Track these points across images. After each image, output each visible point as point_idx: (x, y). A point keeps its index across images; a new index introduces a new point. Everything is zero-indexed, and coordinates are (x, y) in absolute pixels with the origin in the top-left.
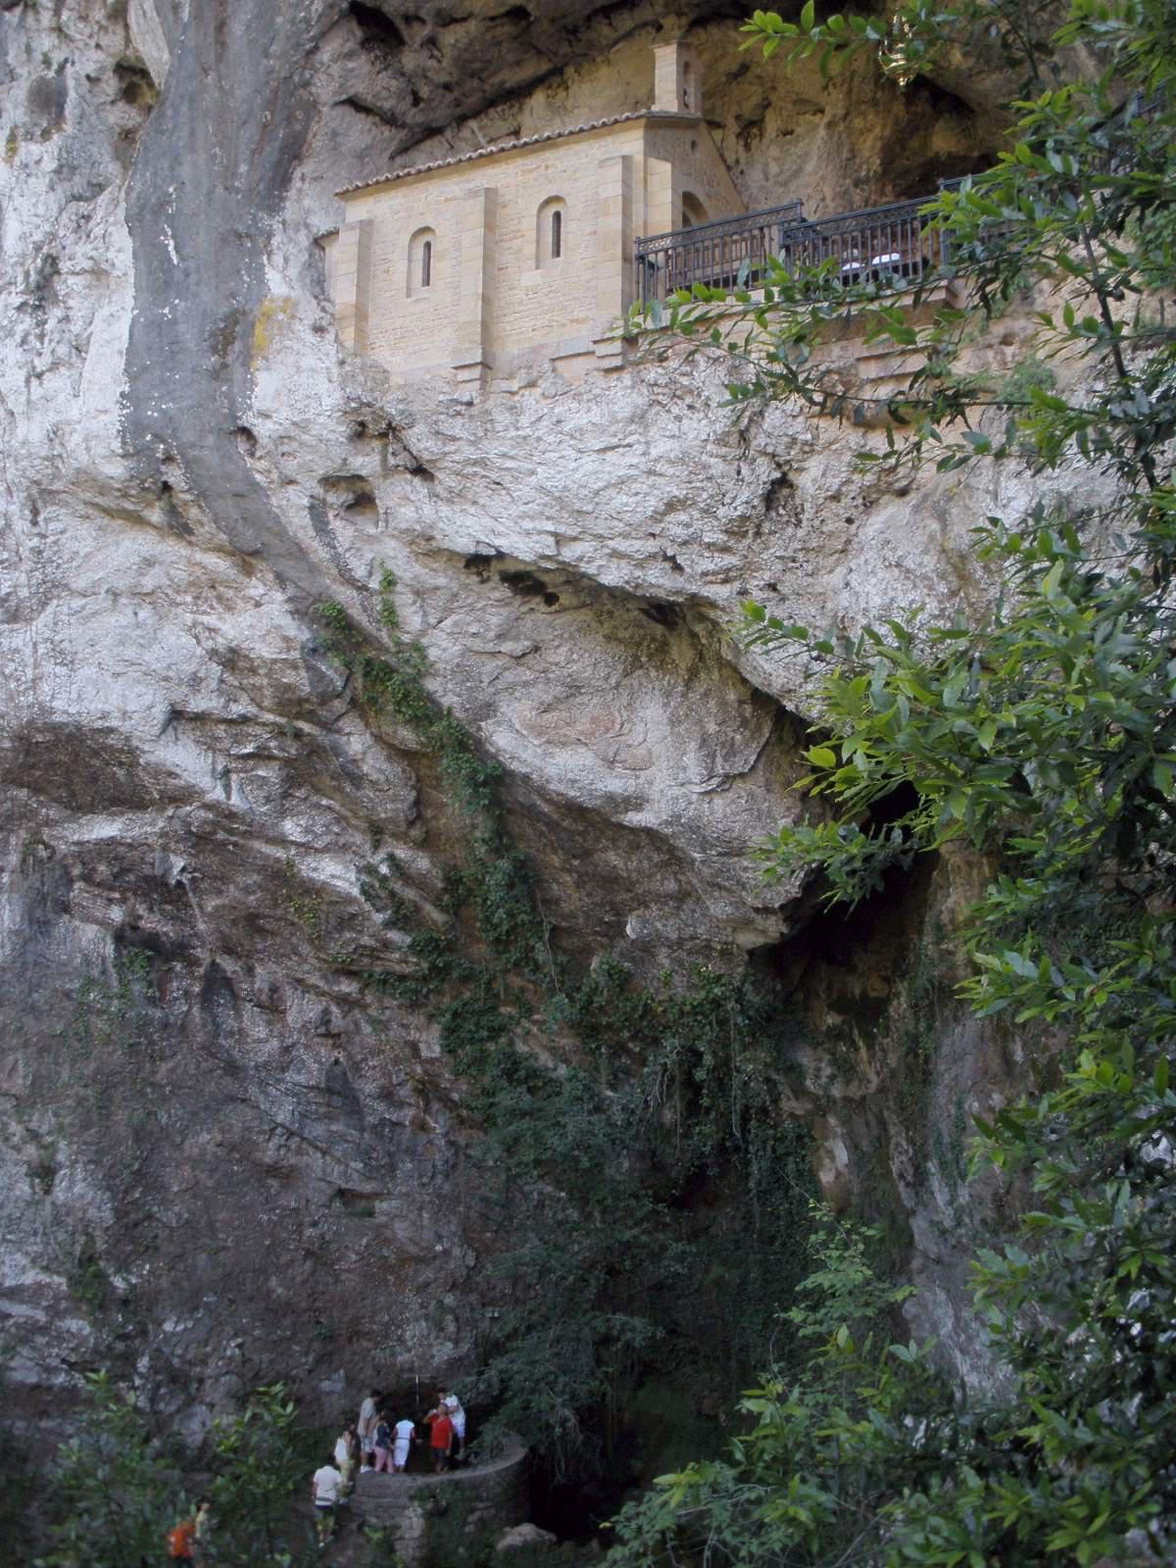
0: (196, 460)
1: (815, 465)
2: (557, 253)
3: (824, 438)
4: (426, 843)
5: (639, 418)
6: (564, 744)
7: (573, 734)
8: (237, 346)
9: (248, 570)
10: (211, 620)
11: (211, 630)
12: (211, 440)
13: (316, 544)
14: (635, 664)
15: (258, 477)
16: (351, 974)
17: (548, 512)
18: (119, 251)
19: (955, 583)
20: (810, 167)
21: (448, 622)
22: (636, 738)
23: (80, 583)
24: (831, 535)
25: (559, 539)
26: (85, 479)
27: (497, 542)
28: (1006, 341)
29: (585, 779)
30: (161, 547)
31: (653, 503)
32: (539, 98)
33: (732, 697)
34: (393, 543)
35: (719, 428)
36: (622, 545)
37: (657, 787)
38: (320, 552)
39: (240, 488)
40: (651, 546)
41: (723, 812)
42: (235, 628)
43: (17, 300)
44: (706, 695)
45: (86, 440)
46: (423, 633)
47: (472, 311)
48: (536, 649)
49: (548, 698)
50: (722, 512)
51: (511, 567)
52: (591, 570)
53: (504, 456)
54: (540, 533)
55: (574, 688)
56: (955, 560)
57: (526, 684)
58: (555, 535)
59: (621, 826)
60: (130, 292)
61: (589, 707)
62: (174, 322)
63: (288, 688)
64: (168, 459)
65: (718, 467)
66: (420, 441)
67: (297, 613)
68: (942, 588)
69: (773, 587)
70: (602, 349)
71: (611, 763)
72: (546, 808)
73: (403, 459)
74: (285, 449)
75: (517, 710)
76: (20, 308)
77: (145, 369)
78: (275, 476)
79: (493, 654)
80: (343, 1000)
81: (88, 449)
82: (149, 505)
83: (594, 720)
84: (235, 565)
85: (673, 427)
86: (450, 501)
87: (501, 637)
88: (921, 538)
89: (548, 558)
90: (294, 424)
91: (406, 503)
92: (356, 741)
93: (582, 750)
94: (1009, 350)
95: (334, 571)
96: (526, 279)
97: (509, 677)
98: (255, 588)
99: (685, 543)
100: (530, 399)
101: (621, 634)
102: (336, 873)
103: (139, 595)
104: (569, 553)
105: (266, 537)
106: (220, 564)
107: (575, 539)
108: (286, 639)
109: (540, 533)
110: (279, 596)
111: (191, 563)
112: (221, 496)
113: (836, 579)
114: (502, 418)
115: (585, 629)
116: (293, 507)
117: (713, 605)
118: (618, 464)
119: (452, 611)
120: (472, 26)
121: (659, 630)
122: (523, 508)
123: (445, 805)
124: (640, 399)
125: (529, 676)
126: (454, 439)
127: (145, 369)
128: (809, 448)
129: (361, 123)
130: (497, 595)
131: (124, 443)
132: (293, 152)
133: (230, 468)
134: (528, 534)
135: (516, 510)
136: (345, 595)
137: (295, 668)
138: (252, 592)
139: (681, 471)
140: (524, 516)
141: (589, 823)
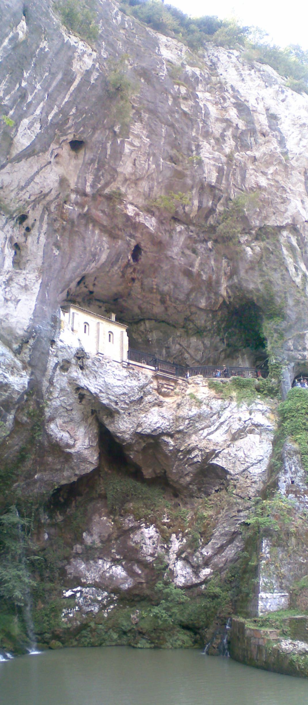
0: (41, 341)
1: (149, 397)
2: (110, 341)
3: (153, 393)
5: (126, 377)
6: (64, 431)
7: (67, 429)
8: (58, 324)
9: (24, 368)
12: (45, 339)
13: (51, 371)
14: (83, 420)
15: (50, 352)
17: (102, 386)
18: (36, 288)
19: (175, 421)
21: (62, 398)
22: (78, 434)
24: (147, 408)
25: (101, 391)
26: (11, 331)
27: (88, 387)
28: (183, 389)
29: (65, 439)
30: (7, 353)
31: (121, 392)
33: (95, 431)
34: (66, 378)
35: (141, 385)
36: (111, 397)
37: (78, 445)
38: (49, 372)
39: (44, 351)
40: (116, 399)
41: (86, 453)
43: (5, 280)
44: (91, 430)
45: (17, 322)
46: (55, 398)
48: (72, 410)
49: (66, 420)
50: (132, 398)
51: (85, 392)
52: (102, 399)
53: (101, 373)
54: (98, 389)
55: (72, 420)
56: (177, 418)
57: (65, 416)
58: (100, 390)
59: (63, 452)
60: (35, 298)
61: (72, 425)
62: (45, 311)
63: (12, 398)
64: (34, 337)
65: (137, 391)
66: (89, 362)
67: (29, 383)
68: (172, 421)
69: (129, 414)
70: (124, 363)
71: (71, 437)
72: (46, 443)
73: (81, 364)
74: (62, 350)
75: (59, 421)
76: (4, 282)
77: (38, 316)
78: (54, 354)
79: (64, 408)
81: (16, 324)
82: (16, 343)
83: (71, 428)
84: (23, 366)
85: (130, 381)
86: (84, 376)
87: (69, 405)
88: (170, 413)
89: (96, 393)
90: (69, 347)
91: (75, 372)
93: (67, 433)
94: (183, 391)
95: (49, 378)
97: (63, 414)
98: (24, 373)
99: (122, 401)
100: (108, 364)
101: (85, 413)
105: (40, 364)
106: (19, 364)
107: (103, 393)
108: (24, 387)
109: (98, 389)
110: (28, 377)
111: (12, 359)
112: (39, 351)
113: (143, 415)
114: (105, 366)
115: (80, 410)
116: (52, 361)
117: (118, 412)
118: (119, 383)
119: (64, 396)
120: (87, 290)
121: (90, 414)
122: (97, 383)
123: (14, 438)
124: (126, 374)
125: (66, 415)
126: (95, 365)
127: (38, 316)
128: (150, 393)
129: (66, 293)
130: (76, 397)
131: (28, 329)
133: (46, 346)
134: (95, 388)
135: (95, 383)
136: (46, 383)
137: (18, 394)
138: (23, 374)
139: (129, 389)
140: (97, 385)
141: (58, 450)
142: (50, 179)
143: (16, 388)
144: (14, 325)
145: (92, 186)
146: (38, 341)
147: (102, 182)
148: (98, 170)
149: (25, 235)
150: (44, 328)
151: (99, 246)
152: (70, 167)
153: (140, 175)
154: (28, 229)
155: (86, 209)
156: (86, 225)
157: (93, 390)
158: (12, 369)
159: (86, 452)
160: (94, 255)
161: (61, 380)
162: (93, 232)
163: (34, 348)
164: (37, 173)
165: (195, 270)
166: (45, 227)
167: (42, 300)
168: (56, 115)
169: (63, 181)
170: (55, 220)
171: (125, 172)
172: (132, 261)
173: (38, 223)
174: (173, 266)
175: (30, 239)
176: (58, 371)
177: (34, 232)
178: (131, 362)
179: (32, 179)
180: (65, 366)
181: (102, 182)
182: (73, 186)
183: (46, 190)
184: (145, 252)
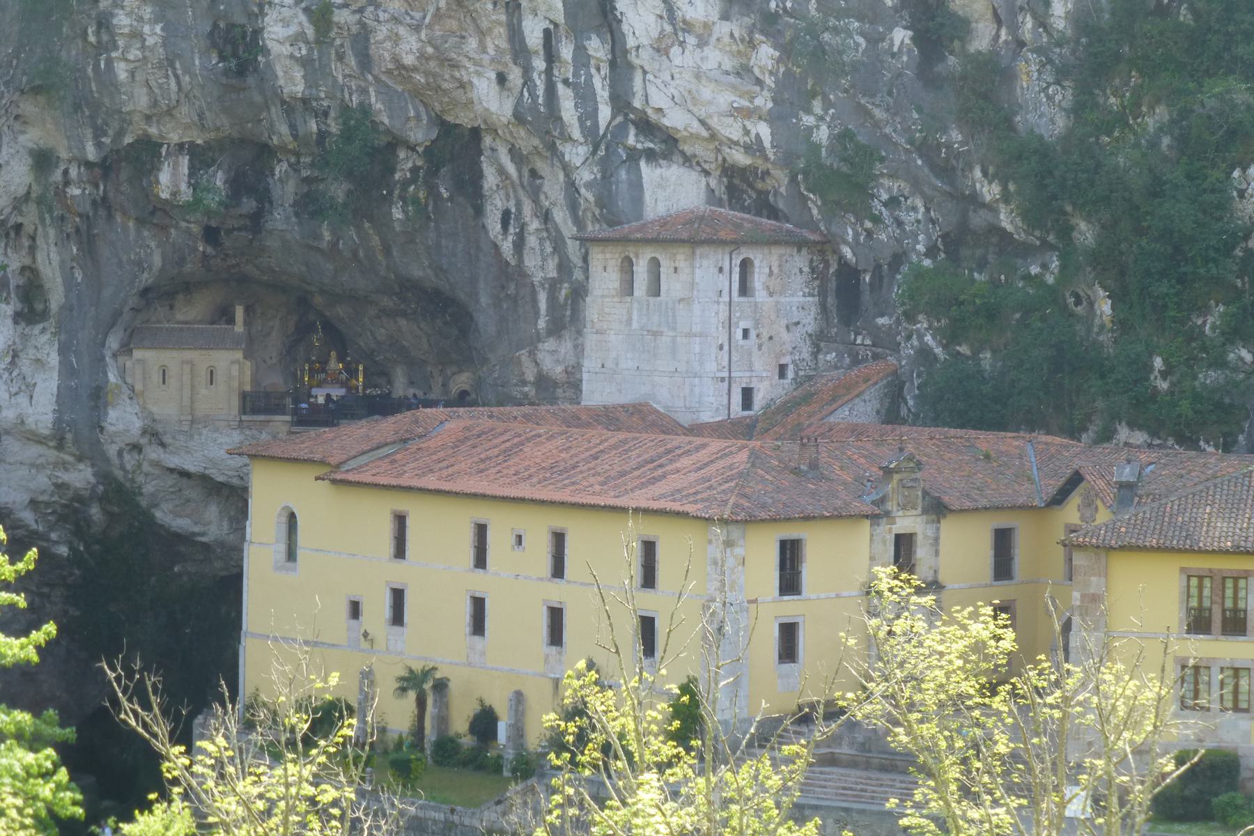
10: (59, 474)
11: (57, 477)
16: (48, 585)
20: (274, 334)
23: (12, 460)
32: (181, 297)
38: (116, 461)
42: (65, 477)
55: (188, 501)
60: (55, 375)
66: (167, 439)
67: (95, 475)
75: (166, 506)
80: (41, 595)
91: (153, 453)
98: (81, 466)
100: (205, 431)
103: (32, 465)
104: (207, 472)
106: (70, 459)
114: (196, 437)
116: (112, 450)
132: (113, 325)
143: (78, 485)
144: (33, 427)
145: (99, 145)
147: (111, 132)
149: (32, 249)
151: (140, 247)
152: (49, 126)
153: (168, 105)
154: (33, 238)
155: (102, 188)
156: (110, 217)
157: (191, 468)
158: (65, 466)
159: (231, 536)
160: (139, 264)
162: (125, 229)
163: (76, 441)
165: (324, 245)
166: (52, 232)
167: (67, 370)
169: (42, 160)
171: (138, 109)
172: (210, 250)
173: (40, 229)
175: (40, 257)
178: (244, 418)
180: (136, 448)
181: (111, 132)
183: (22, 191)
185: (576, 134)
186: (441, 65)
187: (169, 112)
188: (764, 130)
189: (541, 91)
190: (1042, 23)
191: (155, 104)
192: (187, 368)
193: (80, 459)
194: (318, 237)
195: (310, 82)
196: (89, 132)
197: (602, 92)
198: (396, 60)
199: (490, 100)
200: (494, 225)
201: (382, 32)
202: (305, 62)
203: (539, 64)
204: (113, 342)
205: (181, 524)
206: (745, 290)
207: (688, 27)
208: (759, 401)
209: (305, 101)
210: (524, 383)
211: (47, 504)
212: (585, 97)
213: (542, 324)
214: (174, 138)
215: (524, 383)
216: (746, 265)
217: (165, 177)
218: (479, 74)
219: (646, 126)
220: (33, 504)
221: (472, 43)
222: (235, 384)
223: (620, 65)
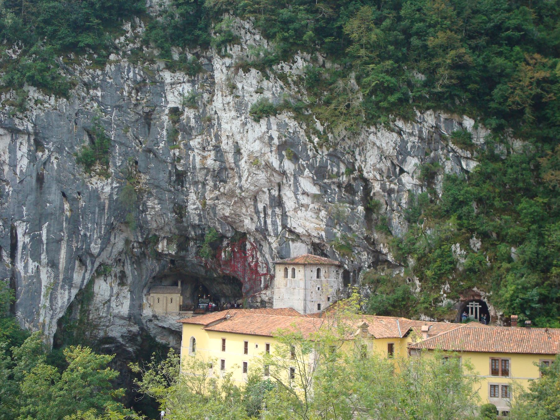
4: (140, 346)
47: (165, 308)
61: (165, 337)
75: (159, 337)
91: (156, 322)
92: (139, 338)
96: (169, 305)
102: (130, 349)
103: (122, 325)
116: (144, 321)
132: (145, 286)
142: (120, 245)
145: (142, 237)
146: (135, 317)
148: (141, 230)
149: (123, 266)
150: (136, 311)
154: (124, 263)
157: (166, 326)
158: (130, 325)
161: (151, 326)
163: (134, 319)
164: (112, 248)
165: (203, 264)
166: (129, 261)
167: (132, 299)
168: (105, 228)
169: (127, 242)
170: (132, 257)
172: (172, 266)
174: (193, 264)
175: (125, 268)
176: (148, 323)
177: (126, 264)
179: (111, 252)
180: (151, 321)
182: (133, 240)
183: (121, 250)
184: (177, 261)
185: (272, 234)
186: (236, 216)
187: (162, 229)
188: (323, 234)
189: (262, 223)
190: (399, 205)
191: (158, 226)
192: (165, 298)
193: (135, 324)
194: (201, 262)
195: (200, 220)
196: (140, 234)
197: (279, 223)
198: (223, 214)
199: (248, 224)
200: (250, 259)
201: (220, 207)
202: (199, 215)
203: (262, 215)
204: (145, 291)
205: (164, 342)
206: (318, 276)
207: (303, 205)
208: (322, 307)
209: (199, 225)
210: (257, 302)
211: (126, 336)
212: (274, 224)
213: (262, 286)
214: (163, 235)
215: (257, 302)
216: (318, 270)
217: (160, 246)
218: (246, 218)
219: (291, 231)
220: (122, 336)
221: (244, 210)
222: (178, 303)
223: (284, 216)
